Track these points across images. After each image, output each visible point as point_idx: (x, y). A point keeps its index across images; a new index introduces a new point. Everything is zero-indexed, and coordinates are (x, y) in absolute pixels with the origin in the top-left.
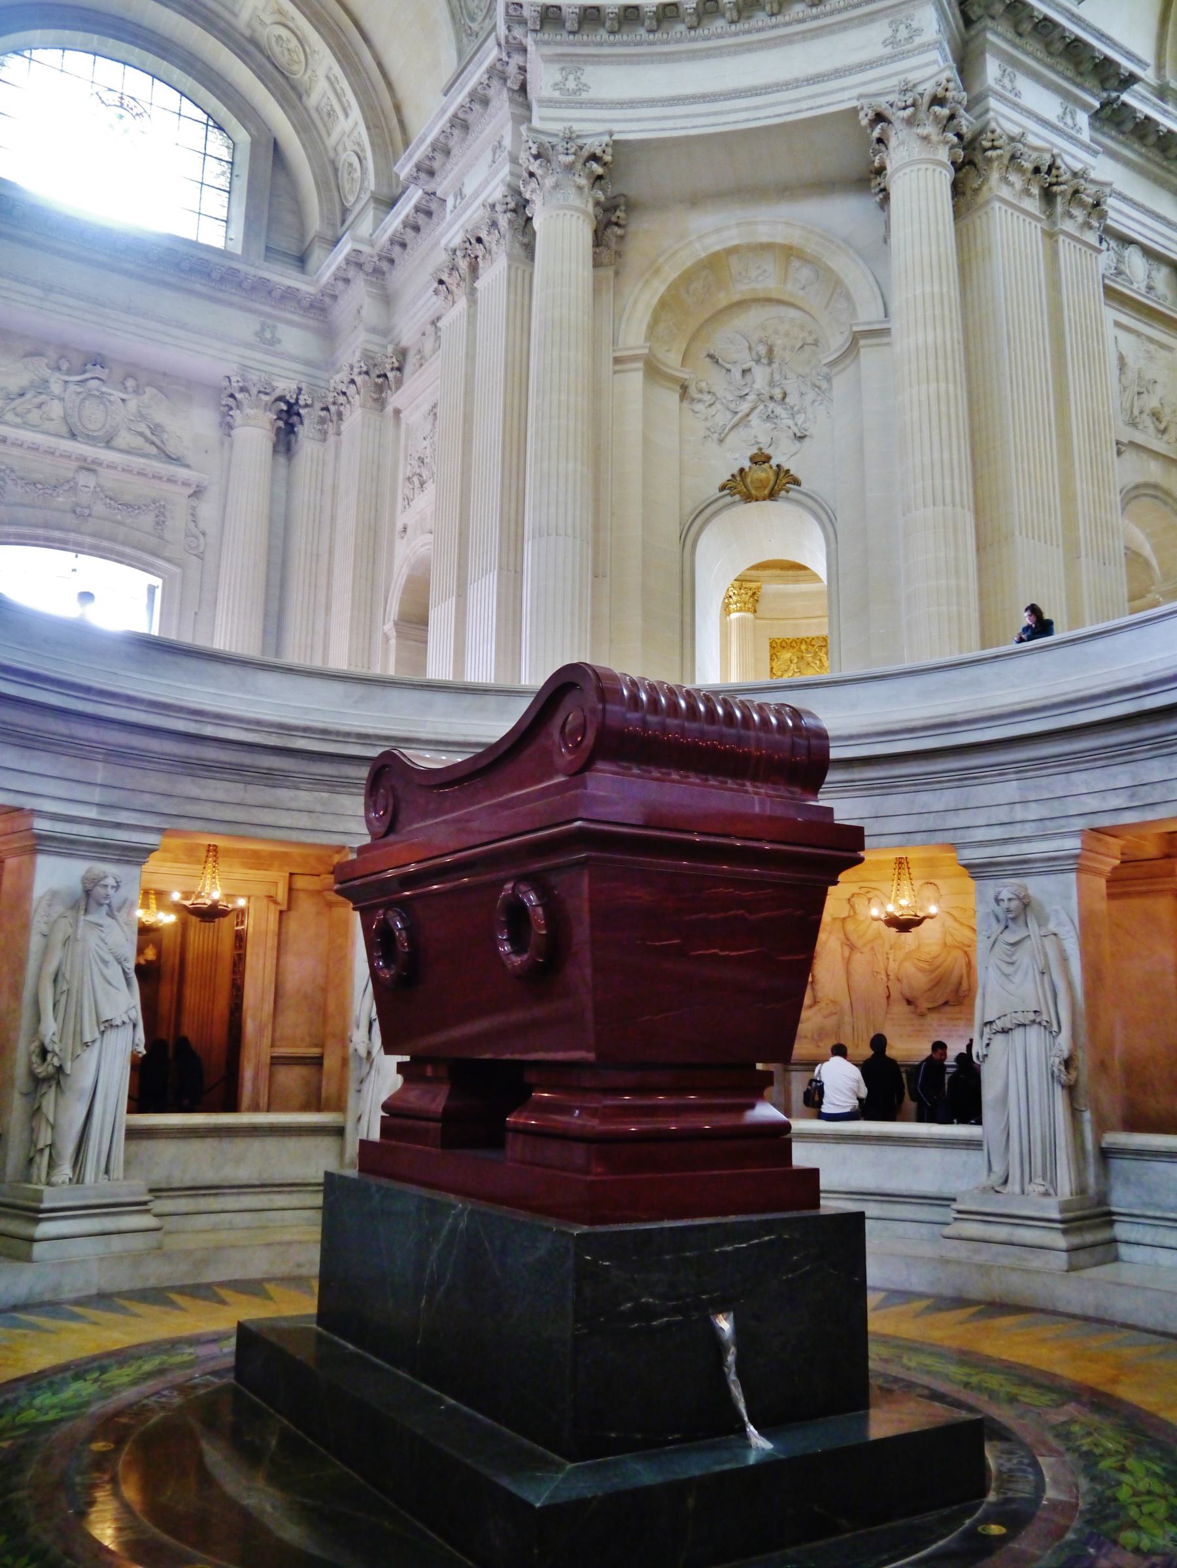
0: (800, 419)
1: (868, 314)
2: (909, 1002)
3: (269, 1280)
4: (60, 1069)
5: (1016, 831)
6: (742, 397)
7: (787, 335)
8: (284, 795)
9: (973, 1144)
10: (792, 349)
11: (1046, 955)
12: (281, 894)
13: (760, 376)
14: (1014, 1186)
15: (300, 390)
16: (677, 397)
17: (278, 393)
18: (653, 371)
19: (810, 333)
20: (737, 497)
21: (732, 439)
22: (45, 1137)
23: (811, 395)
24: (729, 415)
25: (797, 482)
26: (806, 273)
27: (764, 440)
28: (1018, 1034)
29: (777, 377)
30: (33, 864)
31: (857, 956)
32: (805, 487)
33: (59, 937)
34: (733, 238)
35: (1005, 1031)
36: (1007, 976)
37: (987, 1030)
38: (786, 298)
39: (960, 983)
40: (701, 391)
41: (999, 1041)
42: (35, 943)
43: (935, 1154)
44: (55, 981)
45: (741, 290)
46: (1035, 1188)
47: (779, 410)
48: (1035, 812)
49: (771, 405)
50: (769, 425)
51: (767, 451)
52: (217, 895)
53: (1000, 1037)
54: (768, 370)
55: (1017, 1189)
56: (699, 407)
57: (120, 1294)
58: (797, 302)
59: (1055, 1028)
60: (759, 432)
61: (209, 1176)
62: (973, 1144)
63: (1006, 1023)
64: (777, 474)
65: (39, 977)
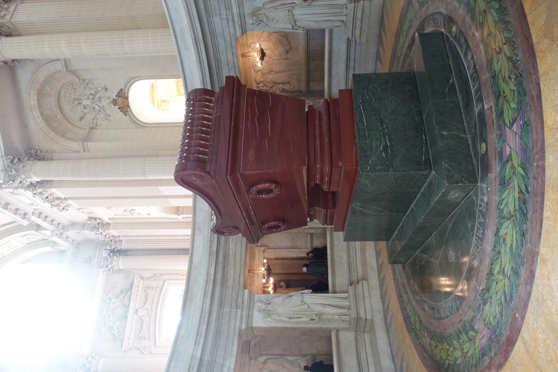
0: (99, 89)
1: (59, 66)
2: (288, 52)
3: (376, 249)
4: (316, 315)
5: (230, 17)
6: (94, 108)
7: (70, 94)
8: (231, 252)
9: (331, 32)
10: (75, 92)
11: (270, 8)
12: (262, 249)
13: (85, 102)
14: (344, 18)
15: (105, 249)
16: (95, 131)
17: (107, 256)
18: (87, 139)
19: (69, 86)
20: (129, 110)
21: (109, 112)
22: (336, 317)
23: (91, 85)
24: (100, 113)
25: (121, 90)
26: (47, 88)
27: (108, 101)
28: (296, 17)
29: (86, 97)
30: (255, 328)
31: (274, 69)
32: (123, 87)
33: (277, 318)
34: (37, 113)
35: (295, 21)
36: (277, 21)
37: (295, 28)
38: (57, 94)
39: (281, 35)
40: (93, 123)
41: (298, 24)
42: (279, 325)
43: (334, 44)
44: (291, 318)
46: (345, 11)
47: (97, 96)
48: (223, 11)
49: (96, 99)
50: (103, 99)
52: (263, 269)
53: (297, 23)
54: (83, 100)
55: (345, 17)
56: (99, 123)
57: (381, 293)
58: (58, 91)
59: (293, 4)
60: (105, 103)
61: (346, 267)
62: (331, 32)
63: (292, 21)
64: (119, 96)
65: (290, 323)
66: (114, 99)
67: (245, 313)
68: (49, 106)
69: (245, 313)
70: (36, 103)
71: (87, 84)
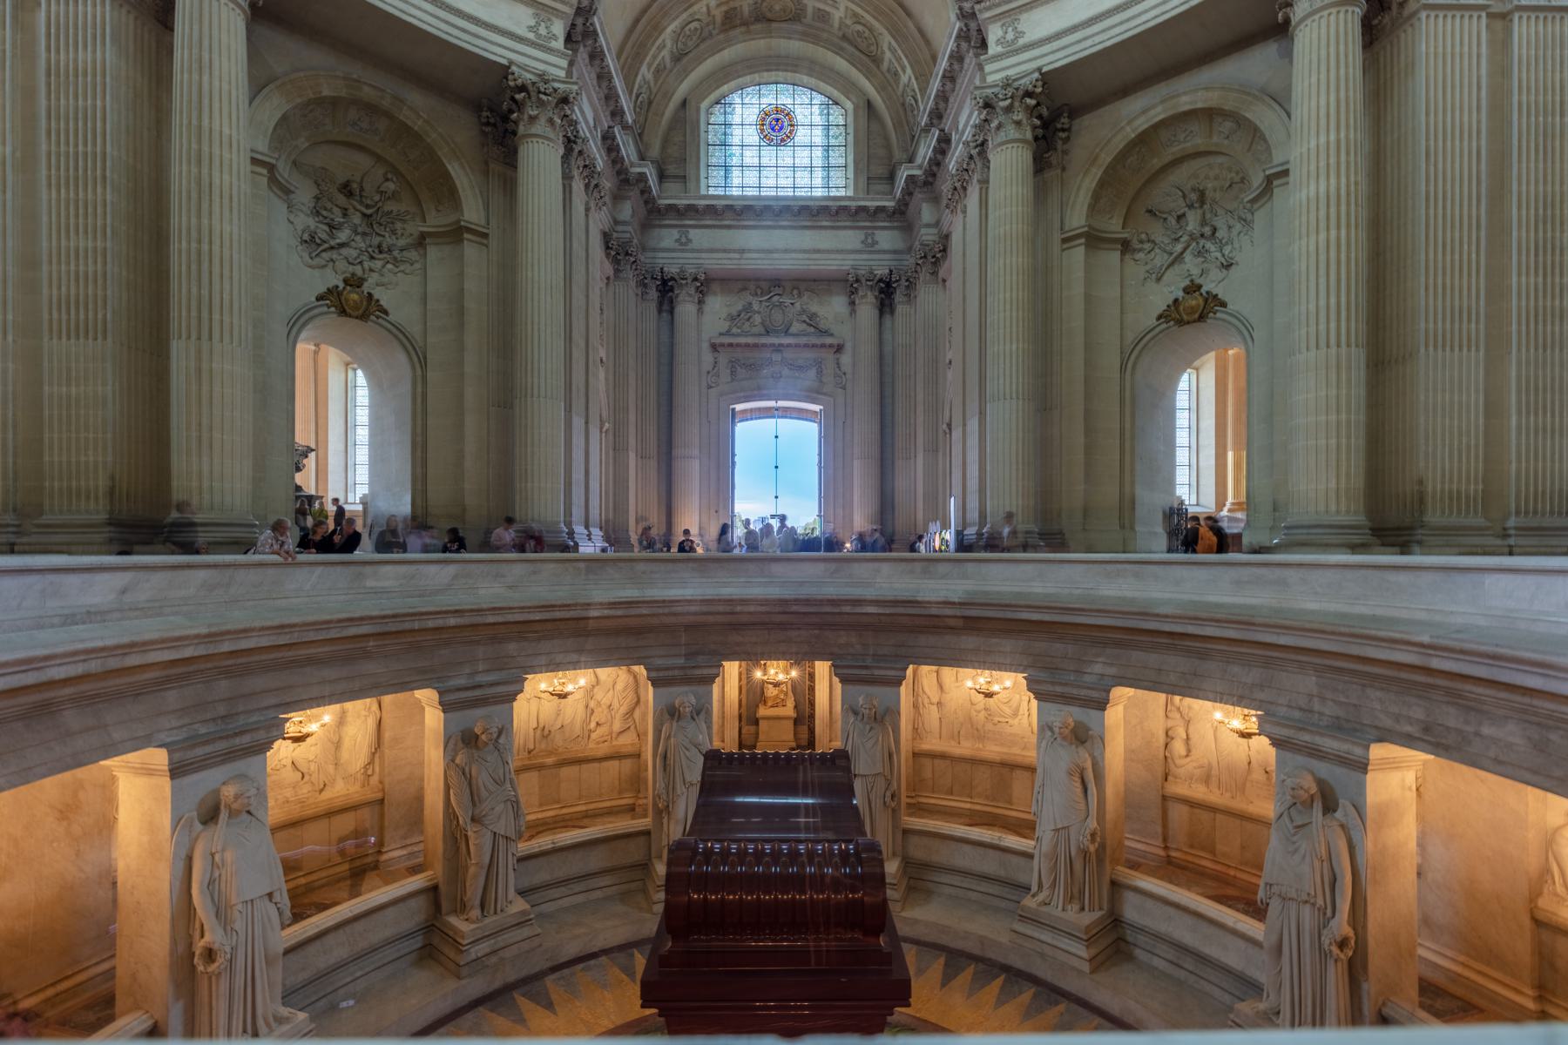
0: (1227, 250)
6: (1177, 240)
7: (1216, 178)
23: (1238, 226)
25: (1223, 304)
27: (1195, 272)
29: (1208, 216)
34: (1158, 114)
38: (1213, 149)
40: (1141, 242)
45: (1174, 151)
47: (1209, 245)
49: (1202, 242)
51: (1198, 281)
54: (1199, 212)
56: (1140, 255)
64: (1206, 300)
66: (1200, 287)
67: (676, 672)
68: (1182, 136)
69: (676, 672)
70: (1187, 108)
71: (1240, 218)
